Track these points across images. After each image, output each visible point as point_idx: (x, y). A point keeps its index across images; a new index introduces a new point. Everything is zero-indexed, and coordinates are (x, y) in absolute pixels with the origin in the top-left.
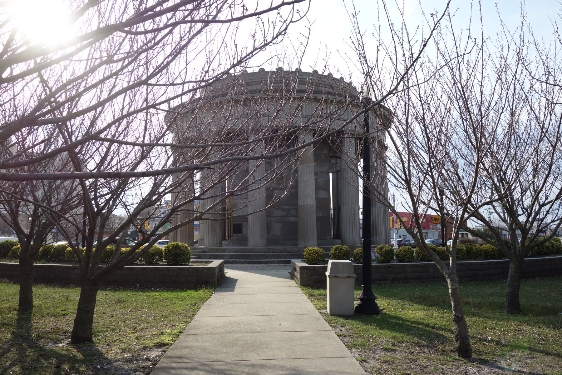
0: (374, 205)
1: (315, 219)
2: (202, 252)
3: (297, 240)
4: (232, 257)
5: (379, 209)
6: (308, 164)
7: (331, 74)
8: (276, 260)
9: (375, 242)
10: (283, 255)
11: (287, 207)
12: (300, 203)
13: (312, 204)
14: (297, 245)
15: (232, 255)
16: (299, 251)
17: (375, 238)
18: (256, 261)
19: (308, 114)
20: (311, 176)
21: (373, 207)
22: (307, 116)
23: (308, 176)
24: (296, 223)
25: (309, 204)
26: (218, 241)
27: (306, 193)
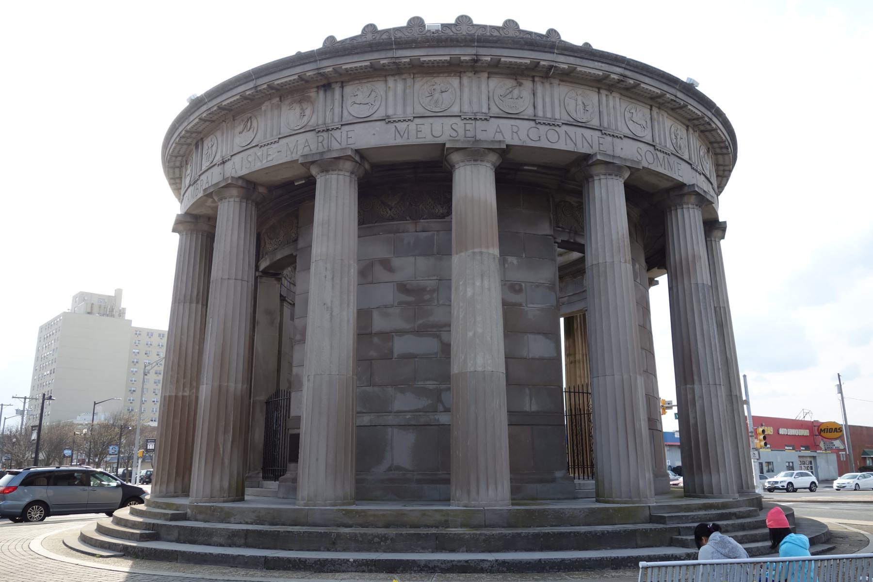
0: (696, 378)
1: (503, 418)
2: (175, 518)
3: (447, 481)
4: (233, 538)
5: (712, 388)
6: (477, 250)
7: (555, 31)
8: (351, 556)
9: (706, 489)
10: (384, 538)
11: (431, 385)
12: (455, 369)
13: (490, 369)
14: (447, 500)
15: (234, 534)
16: (447, 521)
17: (705, 478)
18: (289, 560)
19: (475, 110)
20: (486, 284)
21: (693, 383)
22: (475, 114)
23: (478, 284)
24: (446, 429)
25: (480, 369)
26: (226, 485)
27: (470, 334)
